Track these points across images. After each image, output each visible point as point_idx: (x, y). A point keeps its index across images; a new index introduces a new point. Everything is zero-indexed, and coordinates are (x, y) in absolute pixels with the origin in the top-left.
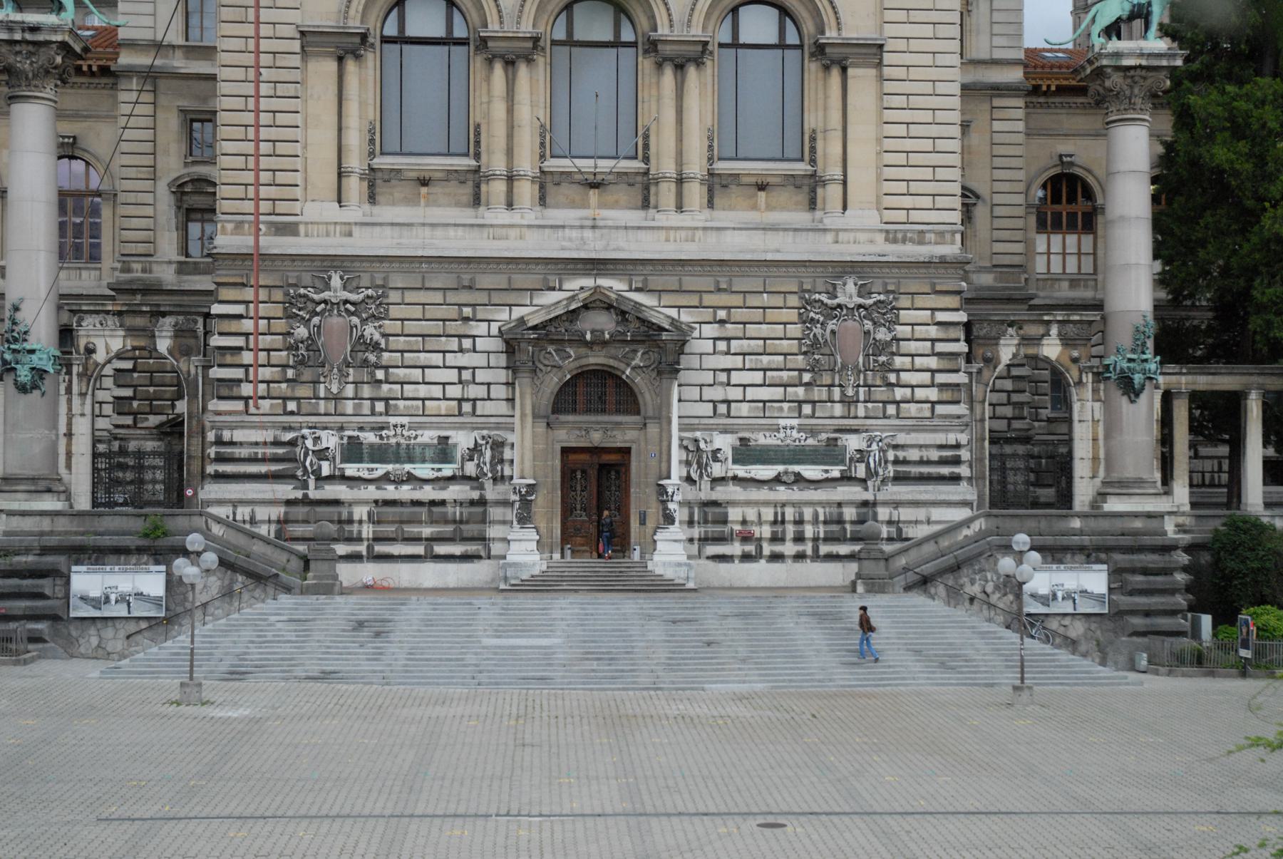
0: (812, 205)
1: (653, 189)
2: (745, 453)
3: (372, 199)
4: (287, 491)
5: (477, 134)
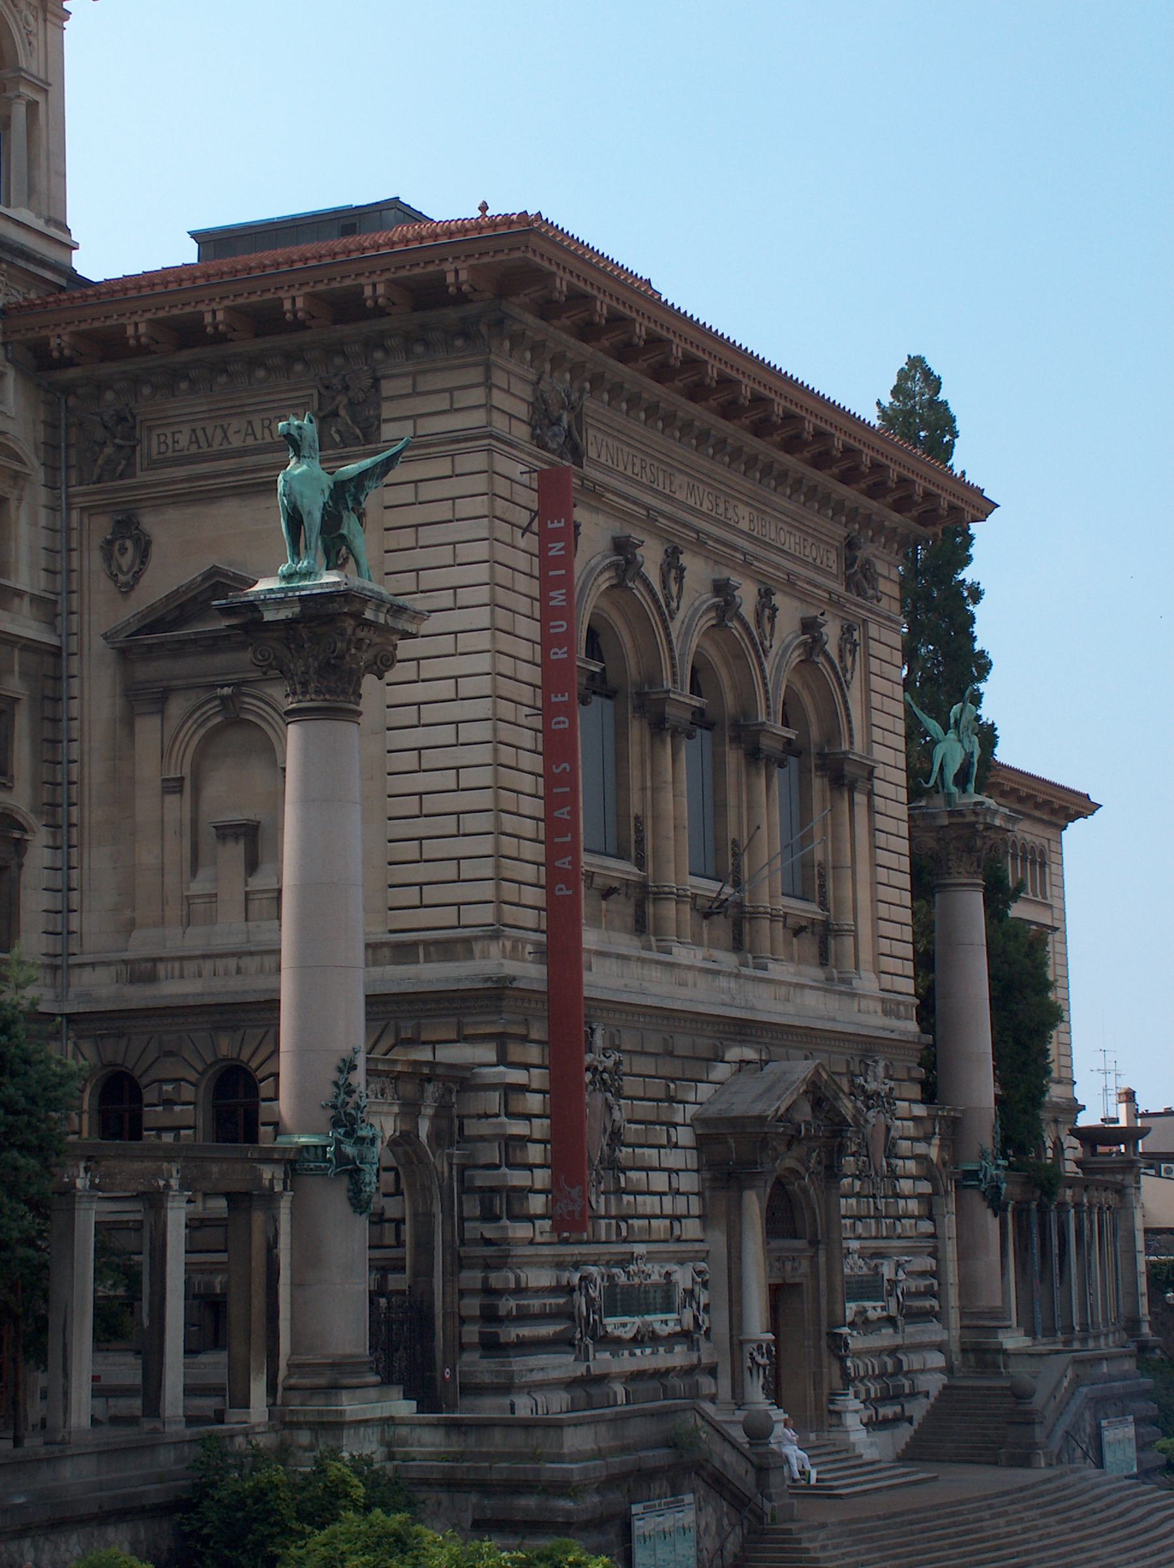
0: (823, 959)
1: (746, 927)
5: (639, 831)
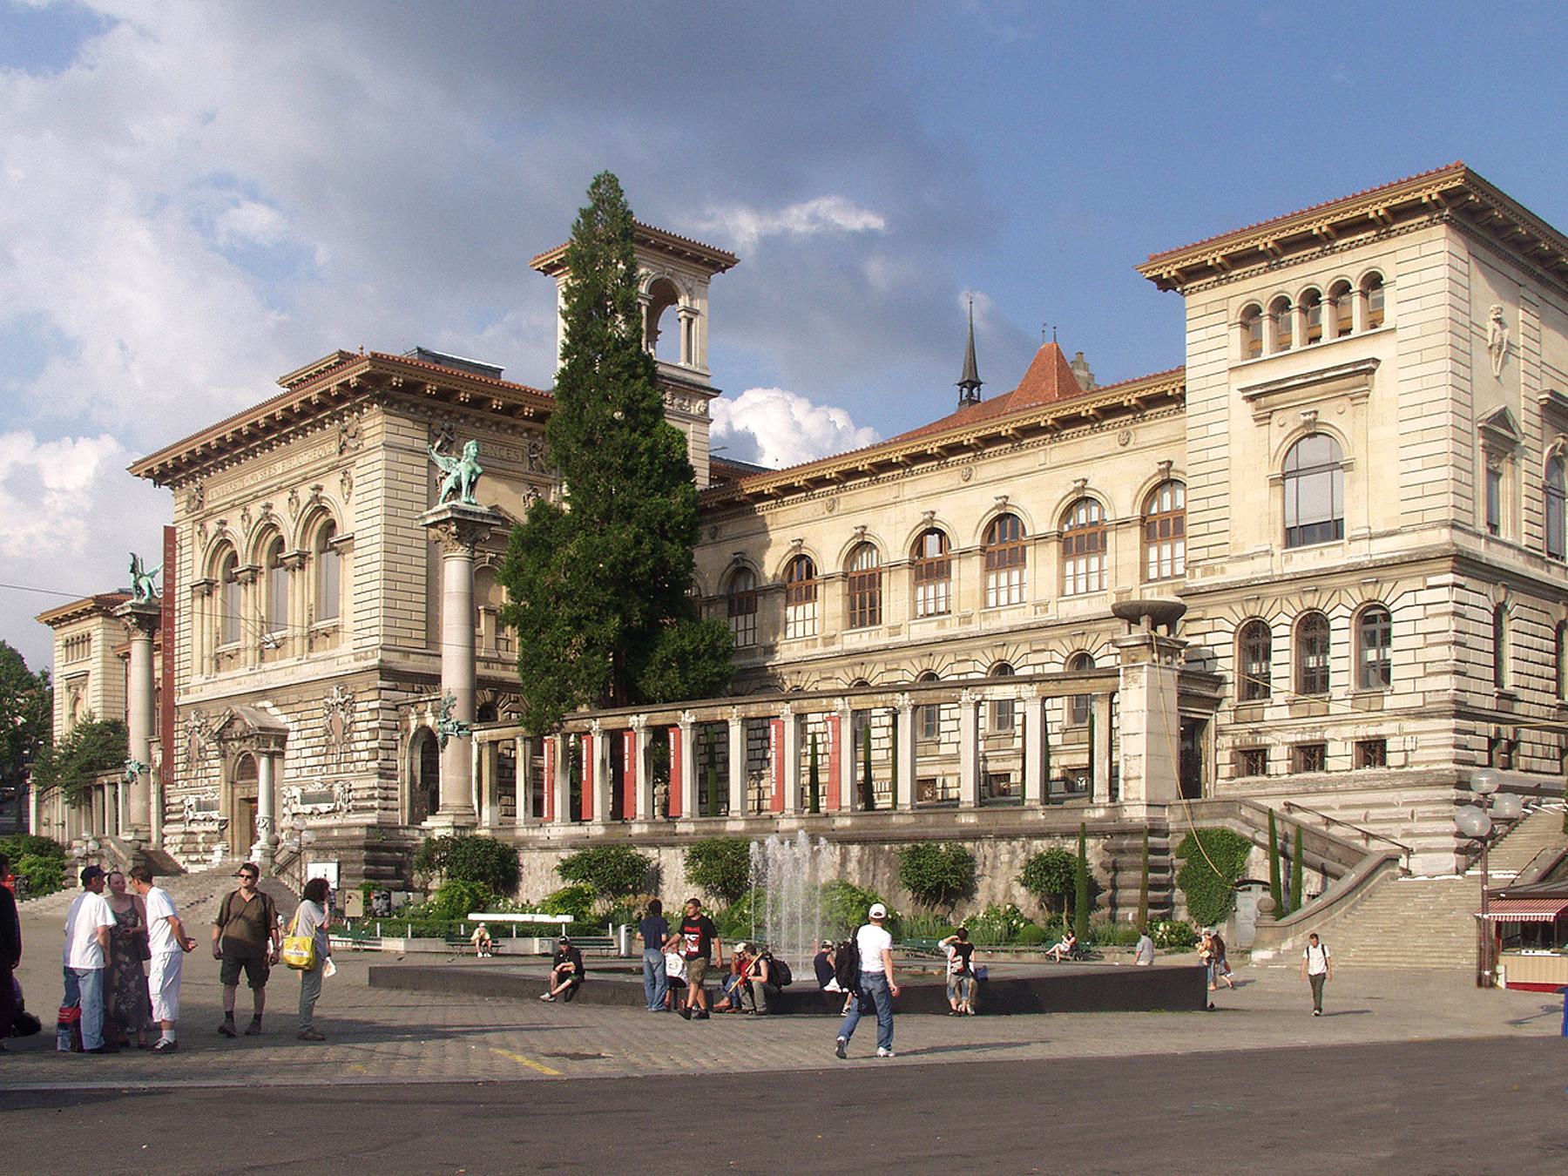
2: (306, 799)
3: (218, 669)
4: (181, 827)
